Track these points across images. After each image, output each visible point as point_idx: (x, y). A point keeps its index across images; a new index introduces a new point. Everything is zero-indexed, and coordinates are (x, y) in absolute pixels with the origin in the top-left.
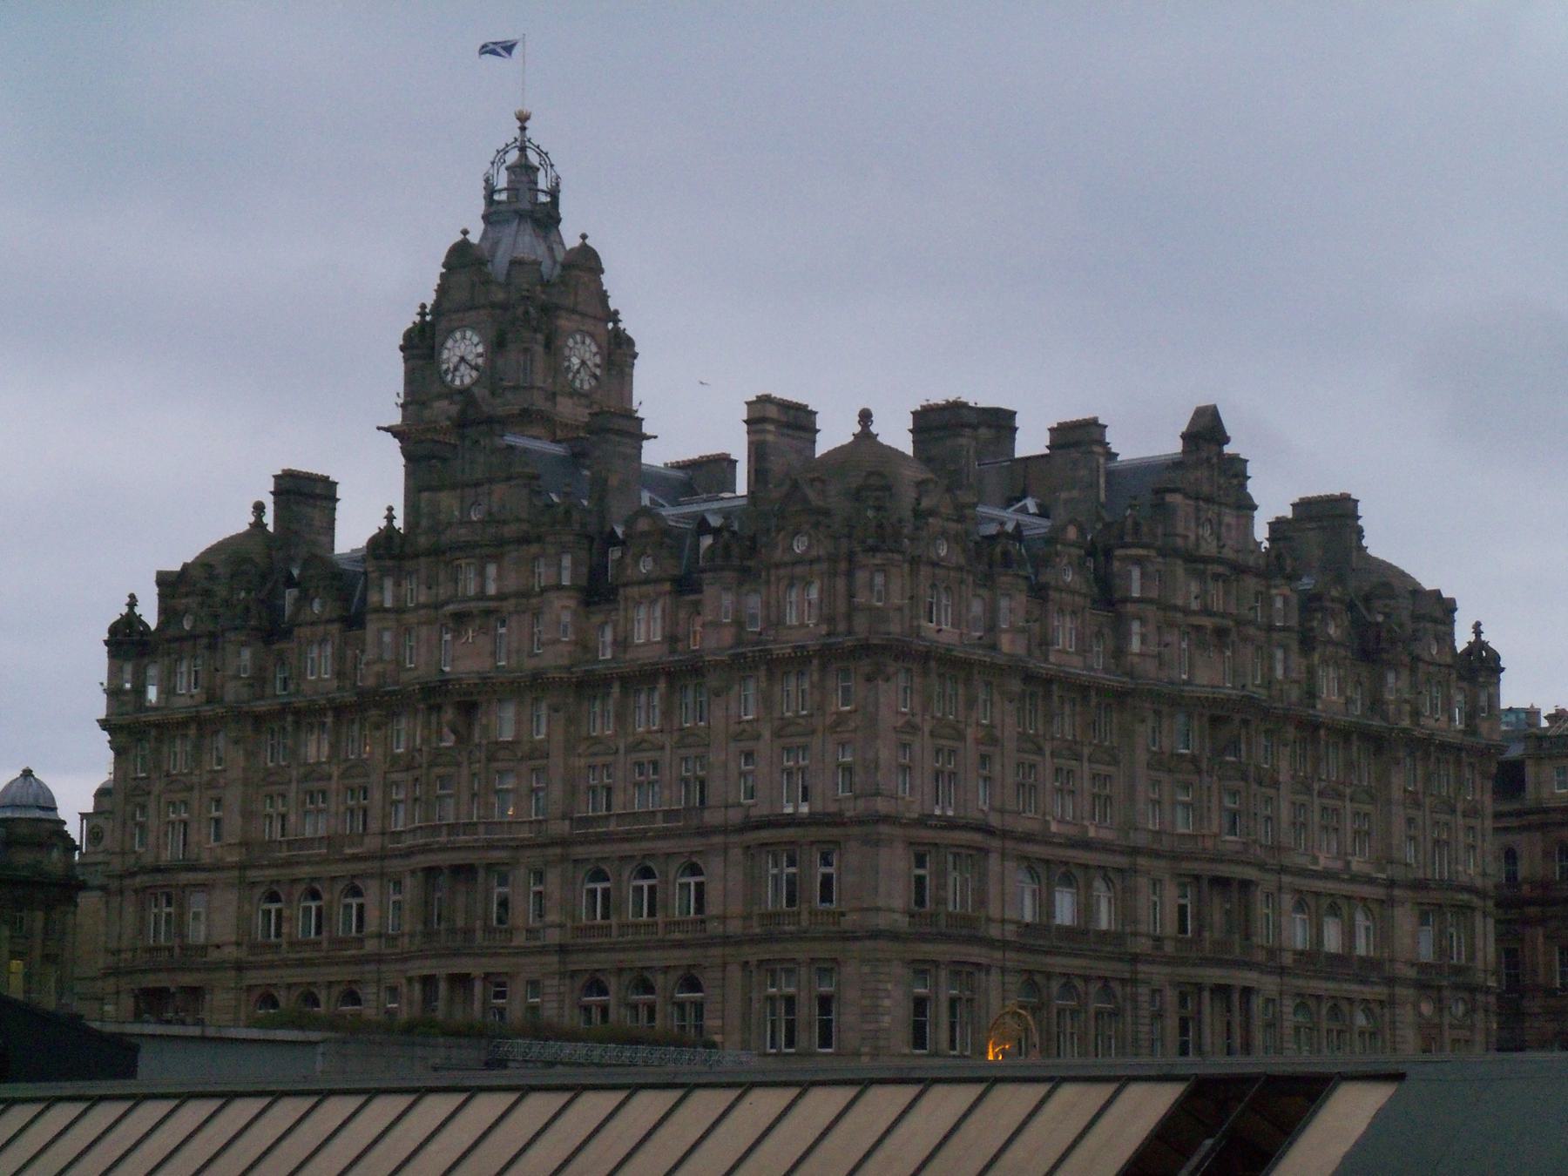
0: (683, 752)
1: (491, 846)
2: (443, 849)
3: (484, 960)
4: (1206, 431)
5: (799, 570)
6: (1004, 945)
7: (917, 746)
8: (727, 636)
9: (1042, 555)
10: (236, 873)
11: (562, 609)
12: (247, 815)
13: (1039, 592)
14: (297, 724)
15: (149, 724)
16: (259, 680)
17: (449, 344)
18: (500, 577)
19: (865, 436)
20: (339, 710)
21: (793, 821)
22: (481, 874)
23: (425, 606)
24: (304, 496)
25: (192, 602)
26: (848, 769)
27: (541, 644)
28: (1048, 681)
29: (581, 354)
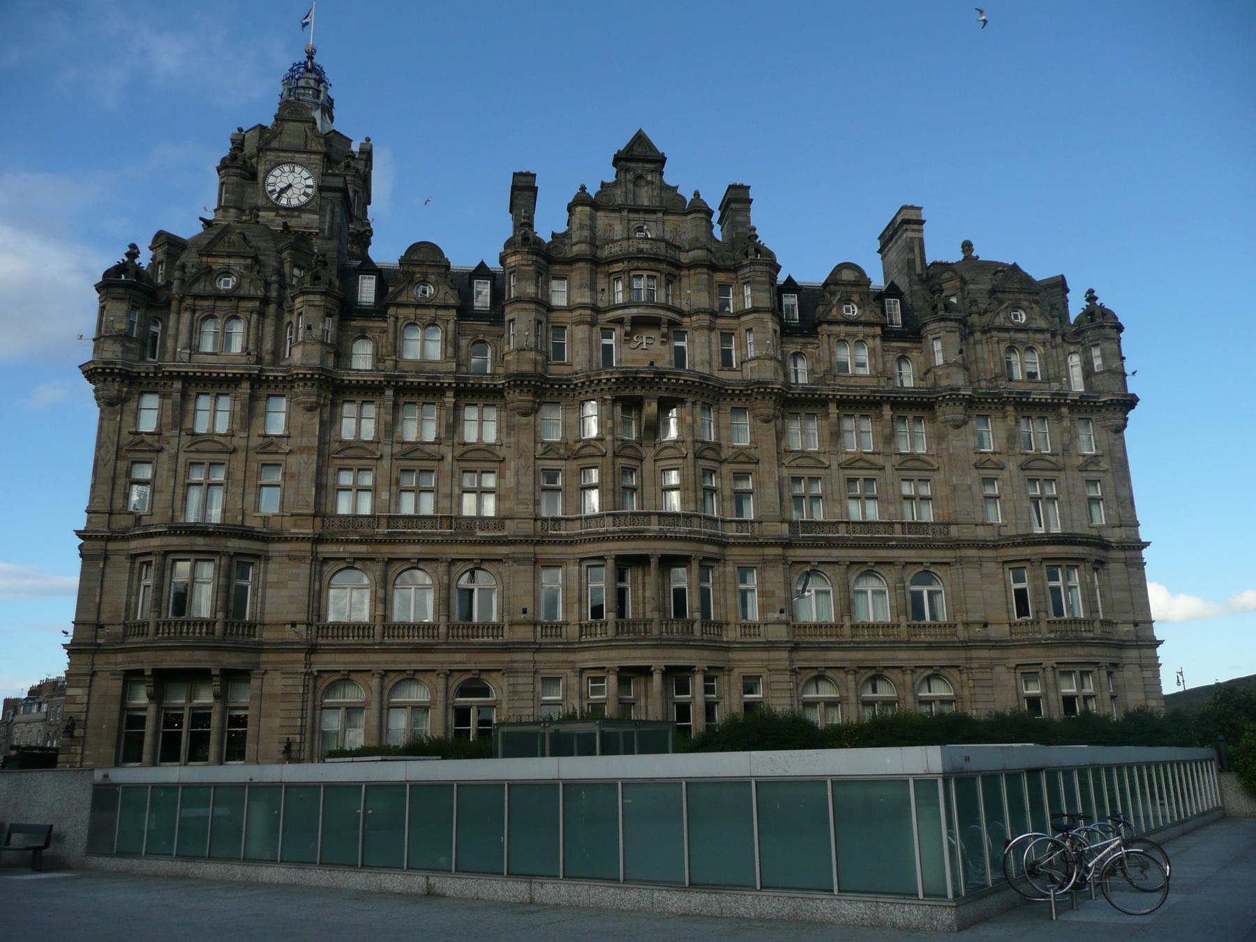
1: (710, 541)
3: (706, 654)
5: (1021, 336)
10: (308, 546)
17: (277, 172)
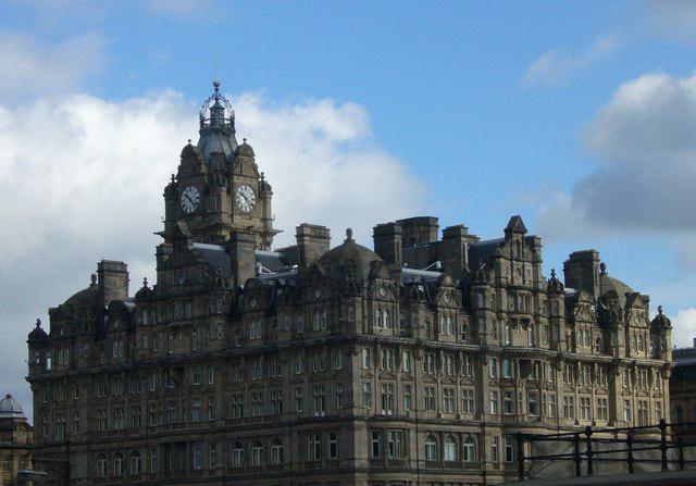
0: (272, 389)
1: (192, 432)
2: (172, 434)
4: (515, 226)
6: (418, 471)
7: (373, 385)
8: (288, 336)
9: (434, 288)
11: (218, 325)
12: (90, 420)
13: (433, 307)
14: (109, 377)
15: (49, 379)
16: (93, 358)
18: (192, 310)
19: (349, 241)
20: (127, 371)
21: (317, 420)
22: (188, 446)
23: (161, 324)
24: (110, 271)
25: (64, 322)
26: (340, 396)
27: (211, 341)
28: (437, 350)
29: (245, 197)
